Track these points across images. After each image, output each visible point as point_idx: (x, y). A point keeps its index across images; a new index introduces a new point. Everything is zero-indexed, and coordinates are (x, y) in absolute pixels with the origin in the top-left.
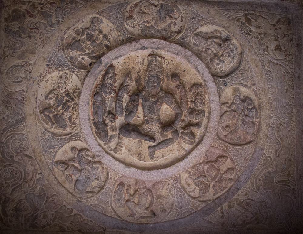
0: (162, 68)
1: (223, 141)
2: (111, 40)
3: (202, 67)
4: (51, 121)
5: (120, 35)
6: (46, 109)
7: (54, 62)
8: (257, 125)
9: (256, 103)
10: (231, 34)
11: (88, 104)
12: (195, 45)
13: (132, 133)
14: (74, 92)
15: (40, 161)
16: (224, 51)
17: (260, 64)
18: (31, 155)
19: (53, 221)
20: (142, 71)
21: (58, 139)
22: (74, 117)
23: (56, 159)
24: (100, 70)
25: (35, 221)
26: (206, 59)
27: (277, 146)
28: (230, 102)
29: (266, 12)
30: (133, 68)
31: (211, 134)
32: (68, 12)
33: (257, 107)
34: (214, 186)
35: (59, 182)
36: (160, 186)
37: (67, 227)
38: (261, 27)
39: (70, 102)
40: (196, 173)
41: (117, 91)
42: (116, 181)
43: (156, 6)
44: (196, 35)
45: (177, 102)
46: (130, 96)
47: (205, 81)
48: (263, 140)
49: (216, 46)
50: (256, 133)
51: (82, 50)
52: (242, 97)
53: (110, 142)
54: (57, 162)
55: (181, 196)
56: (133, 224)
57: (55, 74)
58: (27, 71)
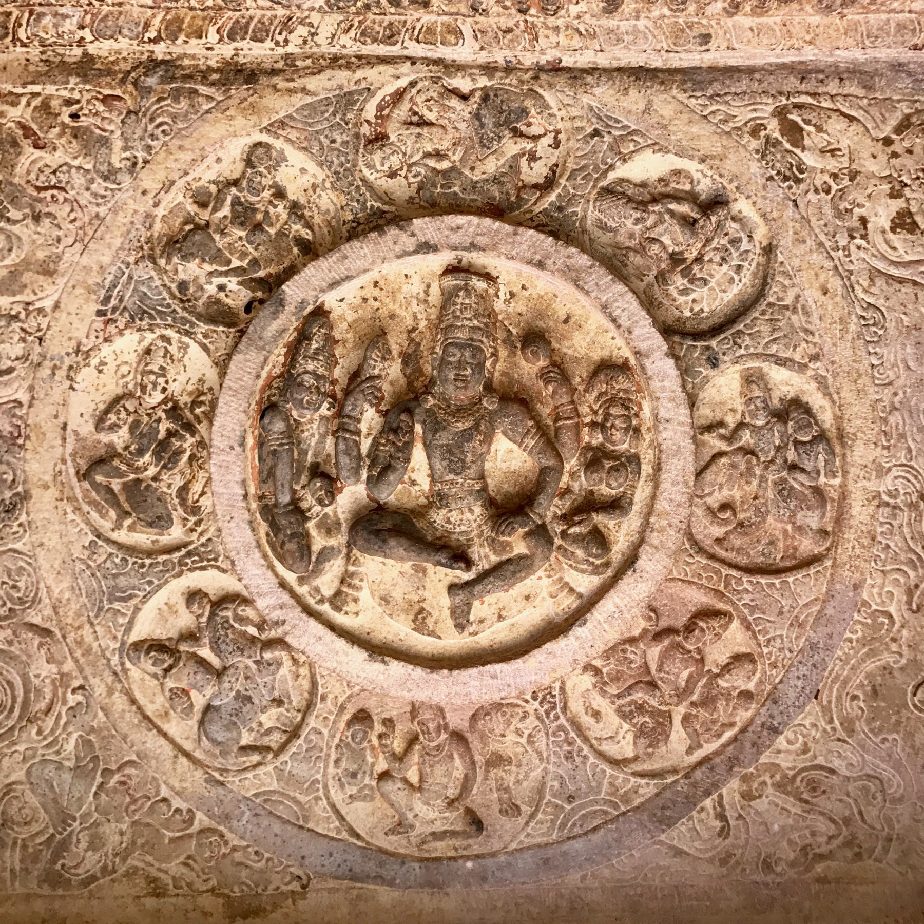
0: (491, 314)
1: (712, 557)
2: (317, 220)
3: (627, 305)
4: (116, 504)
5: (347, 205)
6: (102, 461)
7: (121, 301)
8: (832, 500)
9: (827, 418)
10: (731, 181)
11: (242, 444)
12: (603, 227)
13: (392, 542)
14: (195, 403)
15: (79, 643)
16: (704, 246)
17: (835, 284)
18: (46, 625)
19: (124, 860)
20: (423, 324)
21: (142, 566)
22: (197, 488)
23: (134, 637)
24: (279, 326)
25: (60, 862)
26: (641, 276)
27: (912, 574)
29: (857, 97)
30: (392, 316)
31: (666, 537)
32: (165, 127)
33: (832, 434)
34: (686, 719)
35: (146, 717)
36: (496, 722)
37: (174, 878)
38: (839, 150)
39: (182, 438)
40: (627, 678)
41: (340, 395)
42: (342, 708)
43: (464, 98)
44: (608, 191)
45: (541, 429)
46: (385, 414)
47: (637, 353)
48: (857, 551)
49: (677, 227)
50: (829, 529)
51: (218, 257)
52: (775, 403)
53: (317, 572)
54: (137, 646)
55: (569, 756)
56: (403, 859)
57: (128, 344)
58: (30, 334)
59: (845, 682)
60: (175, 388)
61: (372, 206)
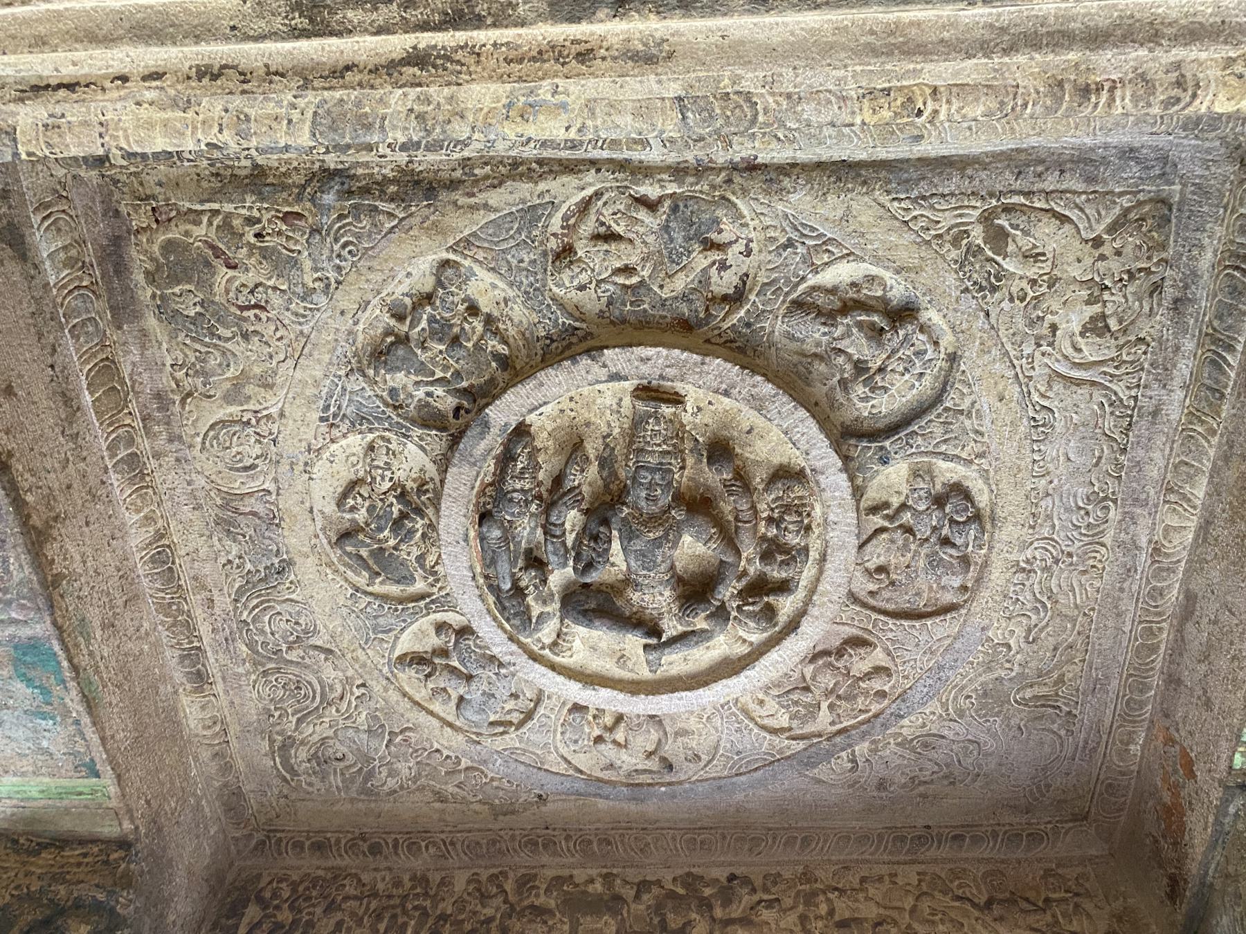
1: (865, 605)
2: (512, 332)
4: (367, 567)
5: (540, 322)
6: (346, 535)
7: (339, 408)
8: (976, 563)
9: (983, 499)
10: (924, 294)
11: (466, 540)
12: (792, 338)
14: (421, 490)
15: (356, 660)
16: (889, 357)
18: (328, 646)
19: (415, 783)
20: (616, 431)
21: (396, 610)
23: (397, 653)
24: (484, 446)
27: (1034, 617)
28: (895, 502)
29: (1074, 192)
30: (588, 424)
32: (351, 248)
35: (417, 703)
38: (1044, 254)
39: (413, 520)
41: (545, 495)
43: (651, 205)
44: (798, 305)
46: (587, 512)
48: (990, 605)
49: (864, 341)
50: (970, 585)
51: (422, 369)
54: (401, 659)
57: (355, 442)
58: (264, 437)
59: (963, 688)
60: (400, 475)
61: (564, 323)
